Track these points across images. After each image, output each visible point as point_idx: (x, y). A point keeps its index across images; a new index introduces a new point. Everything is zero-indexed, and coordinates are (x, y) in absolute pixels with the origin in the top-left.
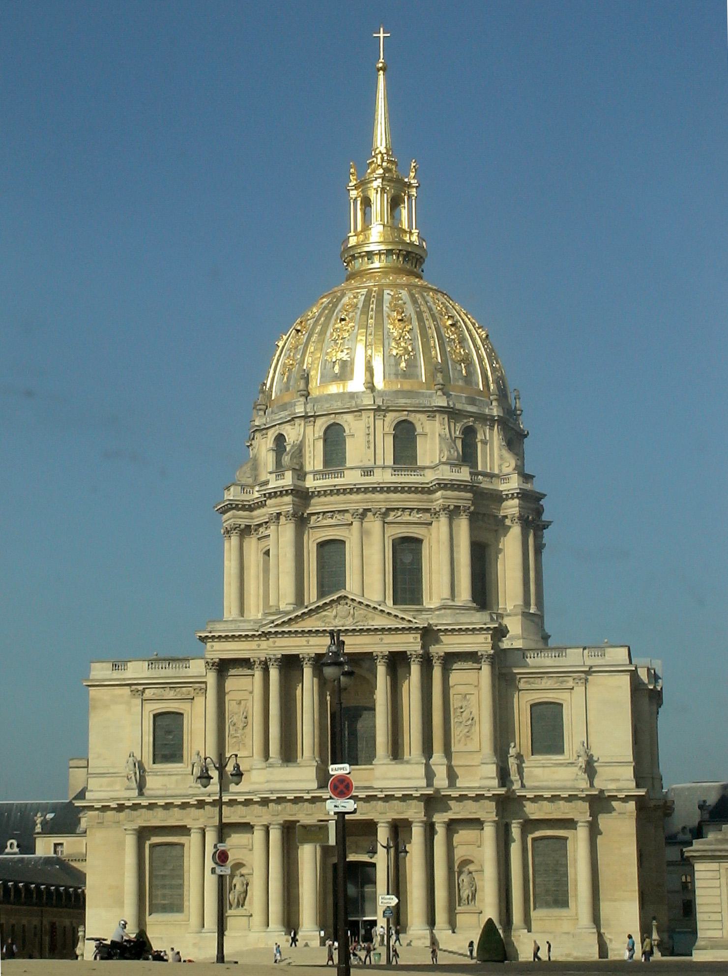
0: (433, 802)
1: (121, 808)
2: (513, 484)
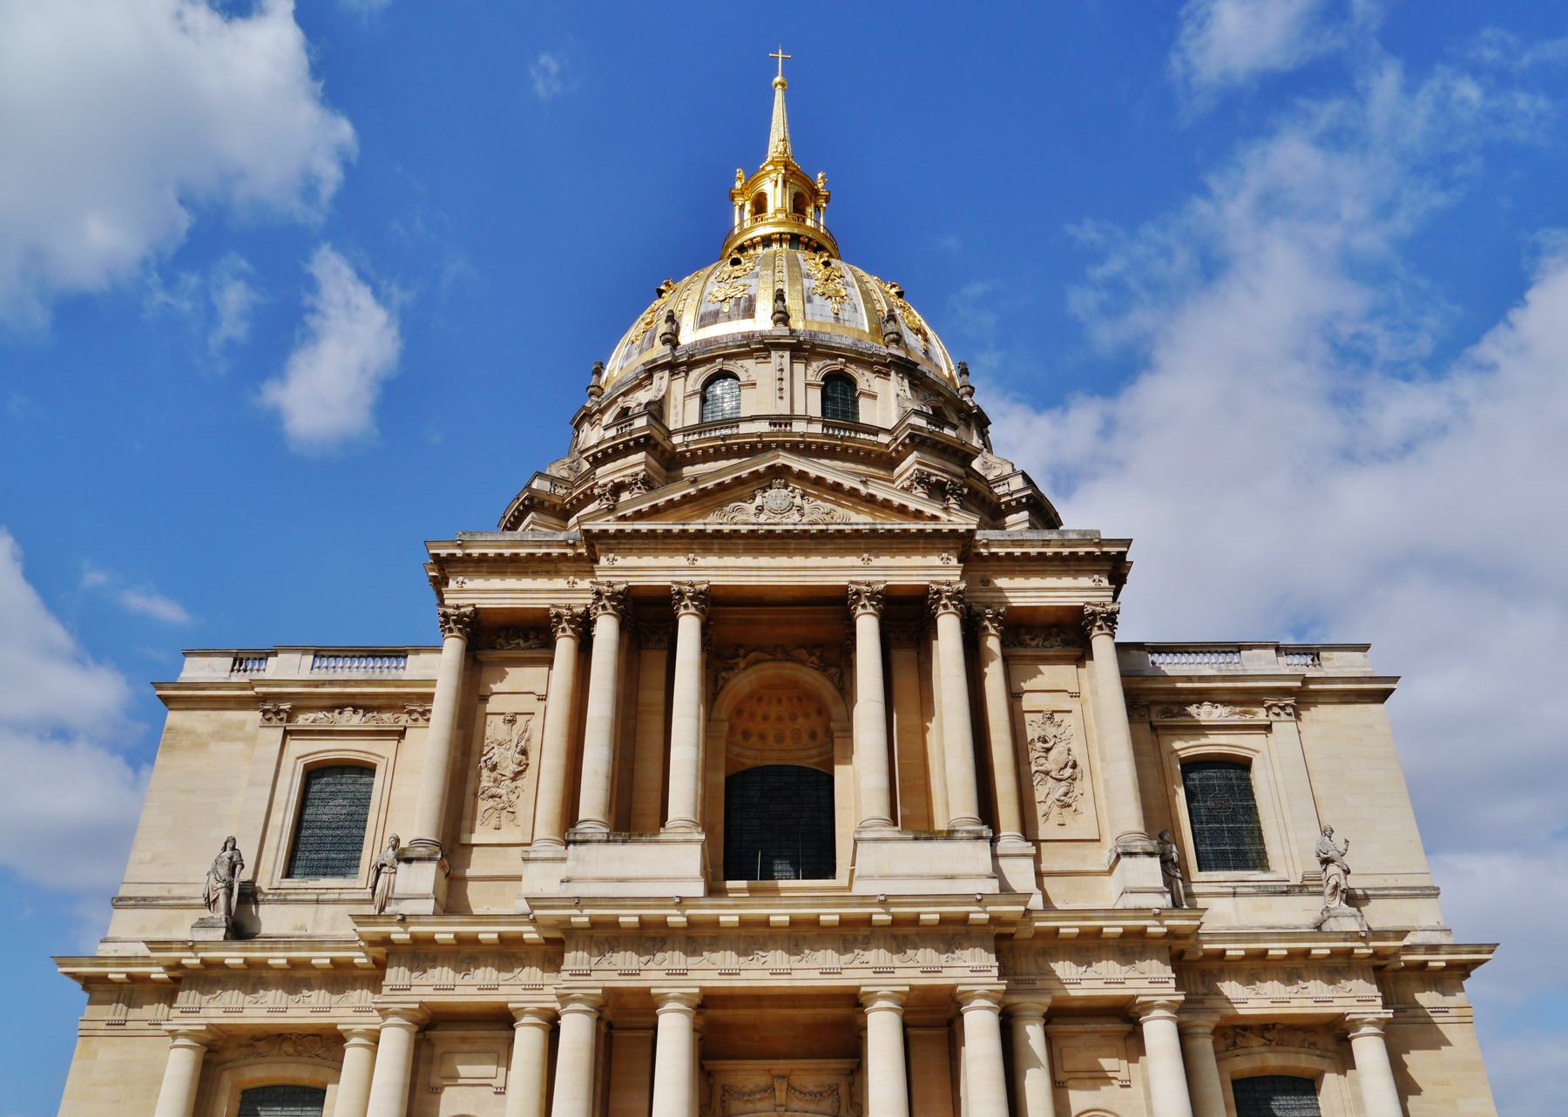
0: (1018, 945)
1: (180, 981)
2: (1017, 483)
